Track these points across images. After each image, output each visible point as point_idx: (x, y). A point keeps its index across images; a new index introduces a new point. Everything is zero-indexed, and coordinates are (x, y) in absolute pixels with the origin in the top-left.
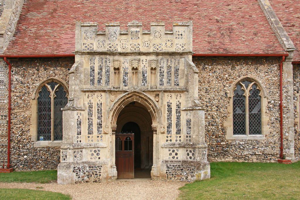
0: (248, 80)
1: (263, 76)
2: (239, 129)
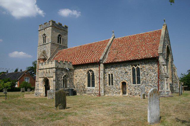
0: (91, 71)
1: (95, 69)
2: (89, 86)
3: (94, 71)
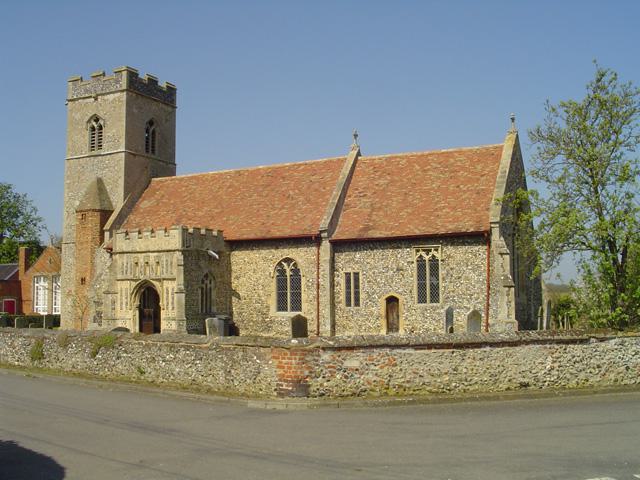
0: (288, 260)
1: (302, 255)
3: (299, 261)
